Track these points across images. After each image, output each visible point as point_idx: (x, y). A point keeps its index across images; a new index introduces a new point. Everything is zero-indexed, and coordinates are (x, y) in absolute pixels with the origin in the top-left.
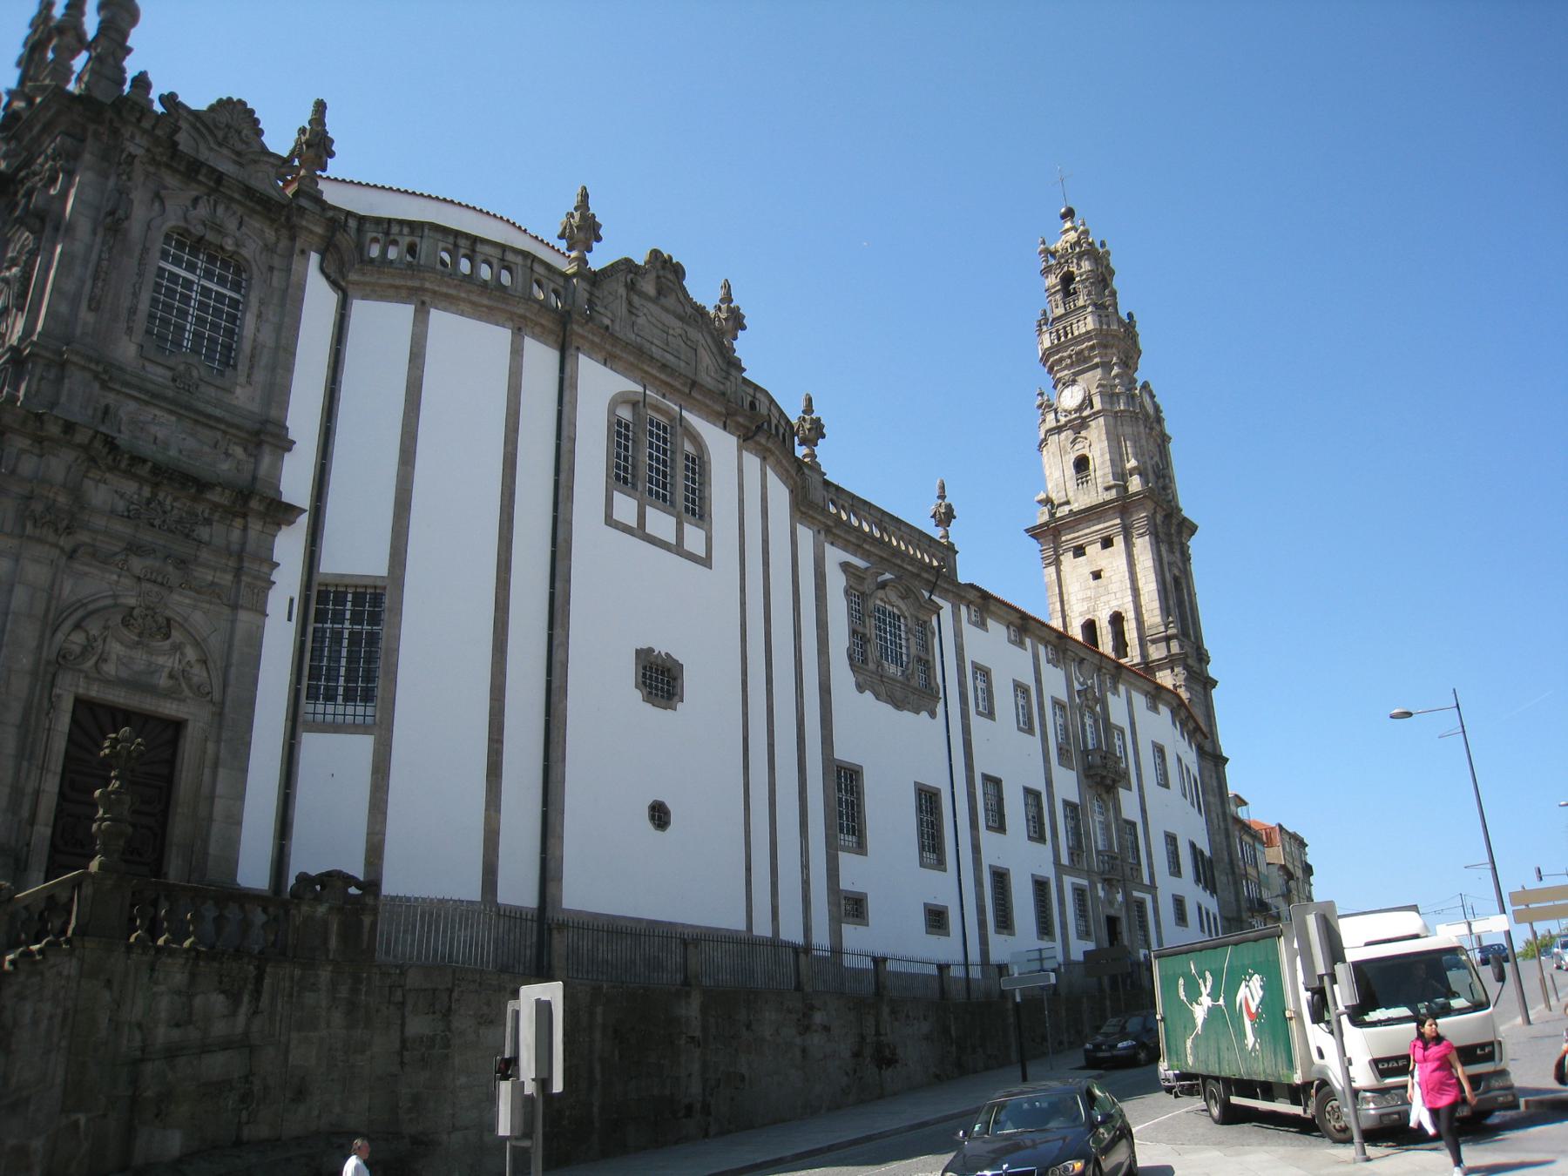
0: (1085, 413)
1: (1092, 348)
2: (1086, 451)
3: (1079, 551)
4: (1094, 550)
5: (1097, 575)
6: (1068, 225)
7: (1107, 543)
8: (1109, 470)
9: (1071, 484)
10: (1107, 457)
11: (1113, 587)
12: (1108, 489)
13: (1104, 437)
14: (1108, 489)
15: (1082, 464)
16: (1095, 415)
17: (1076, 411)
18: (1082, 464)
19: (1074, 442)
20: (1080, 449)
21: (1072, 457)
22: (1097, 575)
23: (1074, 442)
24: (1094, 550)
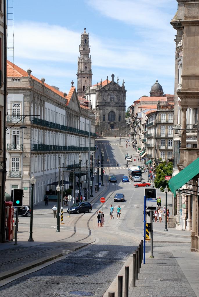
3: (84, 78)
4: (86, 78)
5: (86, 81)
7: (87, 78)
11: (88, 83)
15: (86, 67)
17: (87, 61)
18: (86, 67)
20: (86, 66)
22: (86, 81)
24: (86, 78)
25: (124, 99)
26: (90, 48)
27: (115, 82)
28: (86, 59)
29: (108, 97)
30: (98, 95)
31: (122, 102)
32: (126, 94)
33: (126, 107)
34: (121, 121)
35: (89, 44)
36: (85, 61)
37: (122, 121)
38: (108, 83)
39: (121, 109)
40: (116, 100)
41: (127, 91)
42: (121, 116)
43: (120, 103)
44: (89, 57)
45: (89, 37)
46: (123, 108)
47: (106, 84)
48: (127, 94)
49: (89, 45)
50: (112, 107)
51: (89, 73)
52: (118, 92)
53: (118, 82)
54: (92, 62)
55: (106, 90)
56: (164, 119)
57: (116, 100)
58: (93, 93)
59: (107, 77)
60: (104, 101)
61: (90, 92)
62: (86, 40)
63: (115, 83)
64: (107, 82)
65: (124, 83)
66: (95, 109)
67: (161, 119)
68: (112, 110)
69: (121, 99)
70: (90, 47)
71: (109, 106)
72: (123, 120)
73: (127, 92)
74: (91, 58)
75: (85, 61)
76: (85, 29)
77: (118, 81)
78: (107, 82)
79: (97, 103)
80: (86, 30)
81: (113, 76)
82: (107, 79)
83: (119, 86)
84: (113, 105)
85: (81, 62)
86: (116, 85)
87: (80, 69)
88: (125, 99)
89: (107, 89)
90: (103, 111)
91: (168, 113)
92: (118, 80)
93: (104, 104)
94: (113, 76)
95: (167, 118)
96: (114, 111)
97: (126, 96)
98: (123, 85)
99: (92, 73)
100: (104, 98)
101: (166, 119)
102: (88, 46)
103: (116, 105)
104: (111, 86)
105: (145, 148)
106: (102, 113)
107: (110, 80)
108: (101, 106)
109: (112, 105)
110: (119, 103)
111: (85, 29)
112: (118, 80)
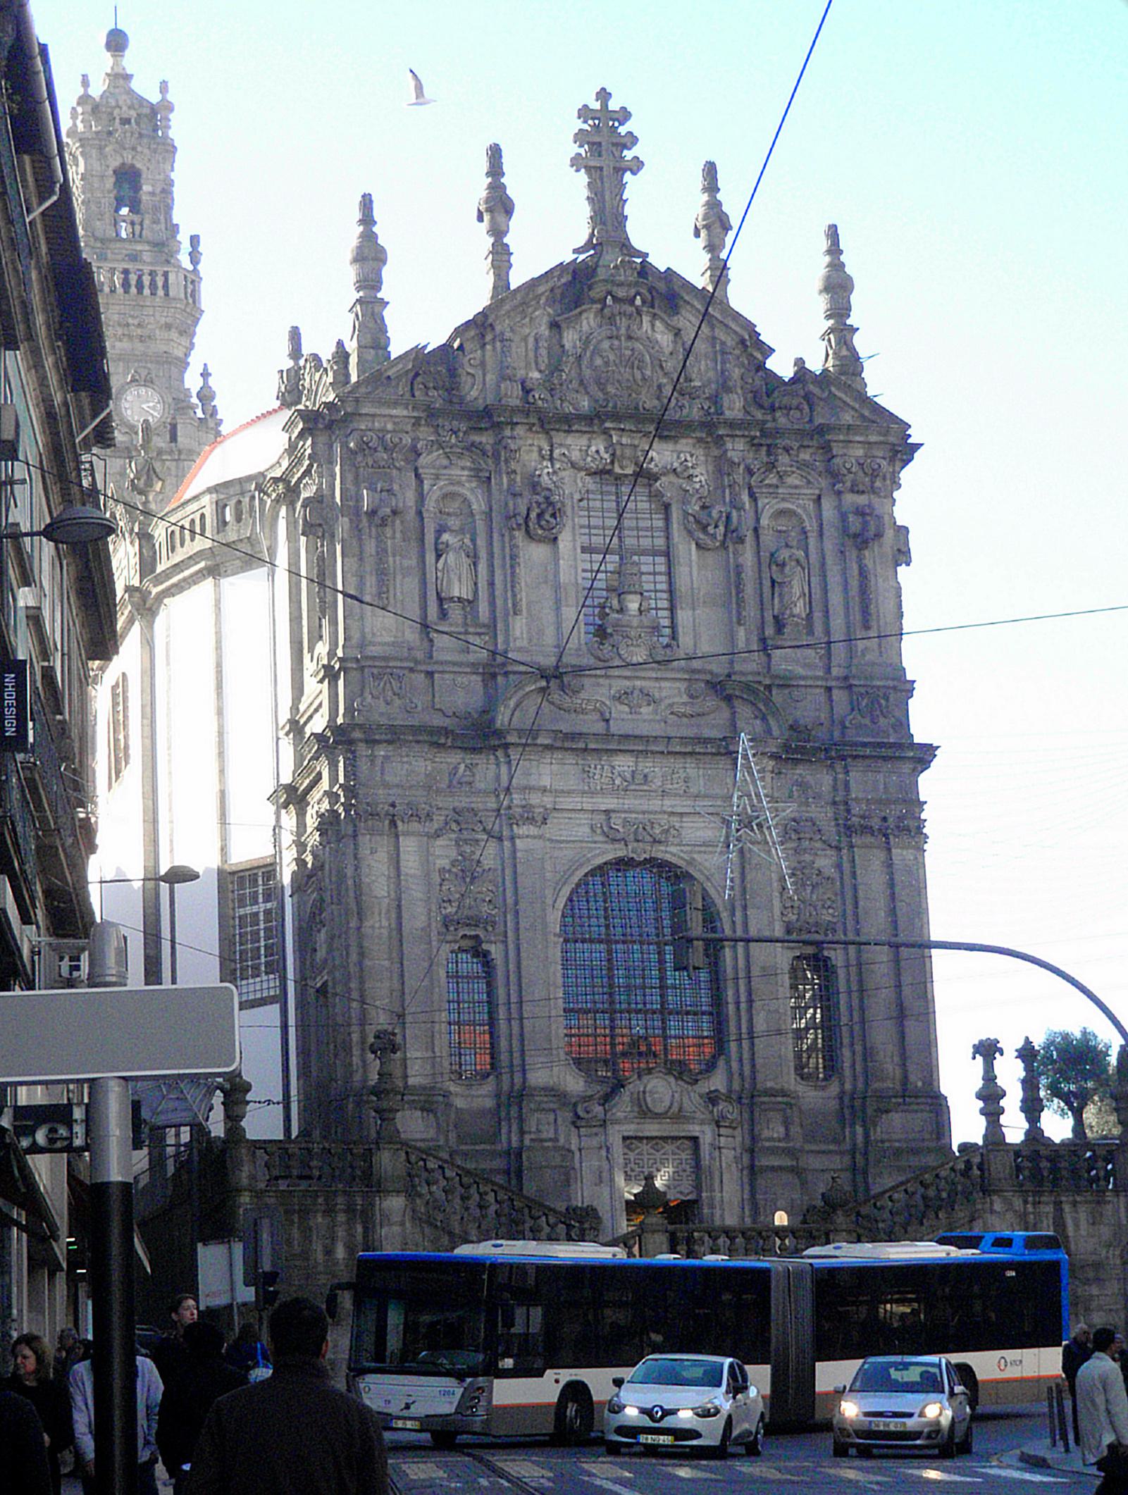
1: (168, 327)
25: (875, 618)
26: (192, 281)
27: (660, 262)
29: (534, 553)
35: (187, 215)
37: (868, 1054)
38: (517, 279)
39: (823, 815)
40: (702, 630)
41: (903, 451)
43: (786, 683)
44: (192, 381)
45: (179, 129)
46: (864, 783)
47: (475, 296)
48: (914, 500)
49: (183, 238)
50: (624, 763)
52: (737, 449)
53: (720, 272)
55: (487, 417)
57: (702, 630)
64: (501, 256)
65: (838, 287)
68: (642, 831)
69: (819, 605)
70: (195, 257)
71: (571, 743)
72: (882, 1035)
74: (206, 396)
76: (117, 41)
77: (713, 247)
78: (501, 256)
80: (130, 61)
81: (606, 148)
82: (498, 206)
83: (752, 346)
84: (646, 721)
86: (687, 321)
88: (887, 607)
90: (444, 852)
92: (715, 225)
93: (463, 694)
94: (606, 148)
96: (670, 853)
97: (902, 555)
100: (459, 589)
102: (164, 246)
104: (570, 338)
106: (415, 892)
107: (551, 233)
108: (395, 736)
109: (623, 720)
111: (117, 41)
112: (715, 225)
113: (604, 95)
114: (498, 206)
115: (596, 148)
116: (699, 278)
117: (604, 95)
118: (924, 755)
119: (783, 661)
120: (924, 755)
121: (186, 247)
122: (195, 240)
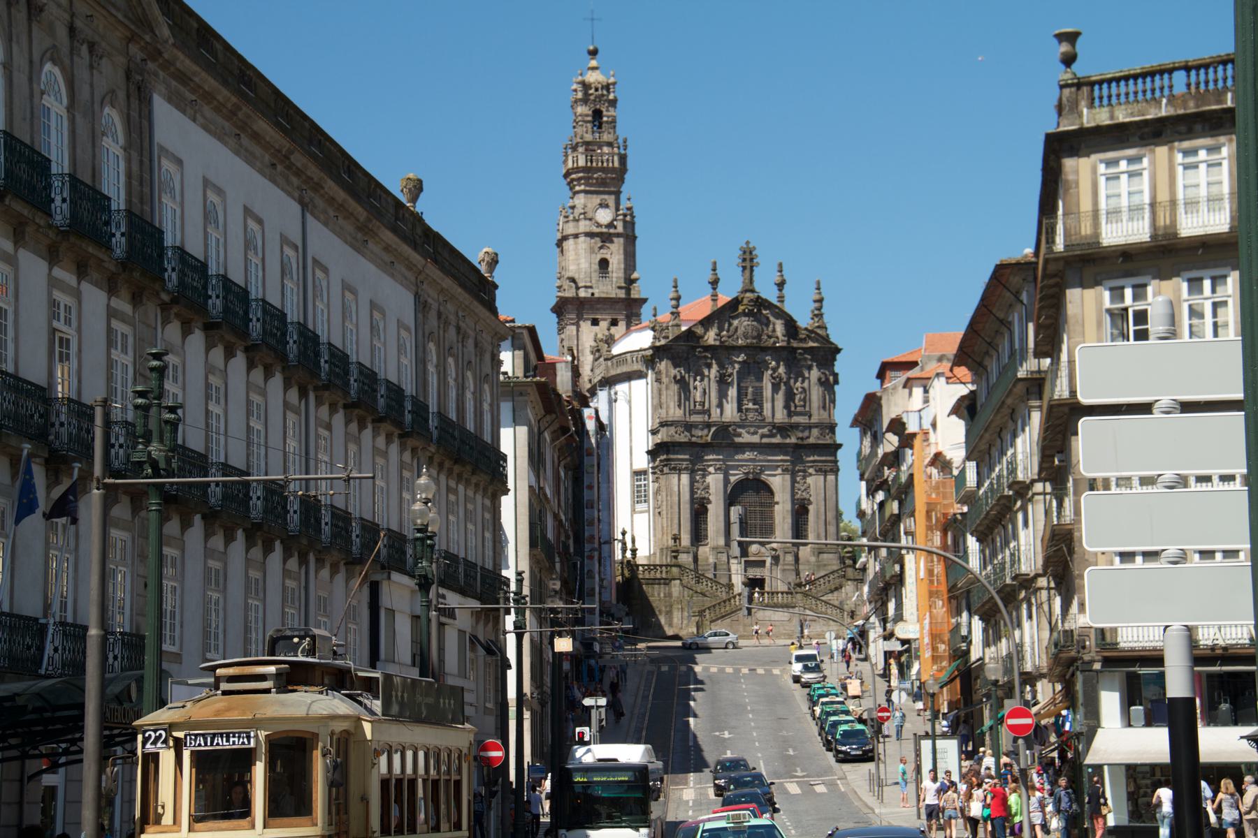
0: (612, 231)
2: (608, 257)
3: (595, 322)
4: (604, 325)
6: (594, 63)
8: (621, 274)
9: (595, 276)
10: (622, 266)
12: (620, 288)
13: (622, 251)
14: (620, 288)
15: (604, 264)
16: (618, 235)
18: (604, 264)
19: (601, 248)
20: (604, 254)
21: (599, 257)
23: (601, 248)
27: (763, 295)
28: (604, 216)
30: (658, 380)
31: (814, 420)
32: (836, 370)
33: (840, 454)
34: (811, 538)
35: (621, 131)
36: (599, 225)
38: (720, 304)
41: (838, 350)
42: (811, 508)
44: (624, 204)
49: (620, 141)
51: (622, 294)
53: (781, 299)
54: (637, 233)
56: (1135, 210)
58: (629, 377)
59: (714, 270)
60: (696, 418)
61: (613, 372)
62: (597, 114)
63: (761, 303)
64: (714, 298)
66: (645, 472)
67: (1096, 212)
73: (838, 357)
75: (596, 230)
78: (714, 298)
79: (654, 432)
81: (748, 260)
82: (714, 283)
84: (755, 439)
85: (576, 236)
87: (570, 274)
89: (711, 337)
91: (1171, 149)
92: (781, 285)
94: (748, 260)
95: (1163, 196)
98: (818, 314)
99: (643, 296)
100: (698, 399)
101: (1153, 205)
103: (774, 440)
105: (964, 632)
109: (746, 437)
110: (795, 427)
112: (781, 285)
113: (748, 243)
114: (714, 283)
115: (744, 260)
116: (774, 301)
117: (748, 243)
118: (840, 446)
119: (795, 419)
120: (840, 446)
121: (620, 141)
122: (625, 141)
